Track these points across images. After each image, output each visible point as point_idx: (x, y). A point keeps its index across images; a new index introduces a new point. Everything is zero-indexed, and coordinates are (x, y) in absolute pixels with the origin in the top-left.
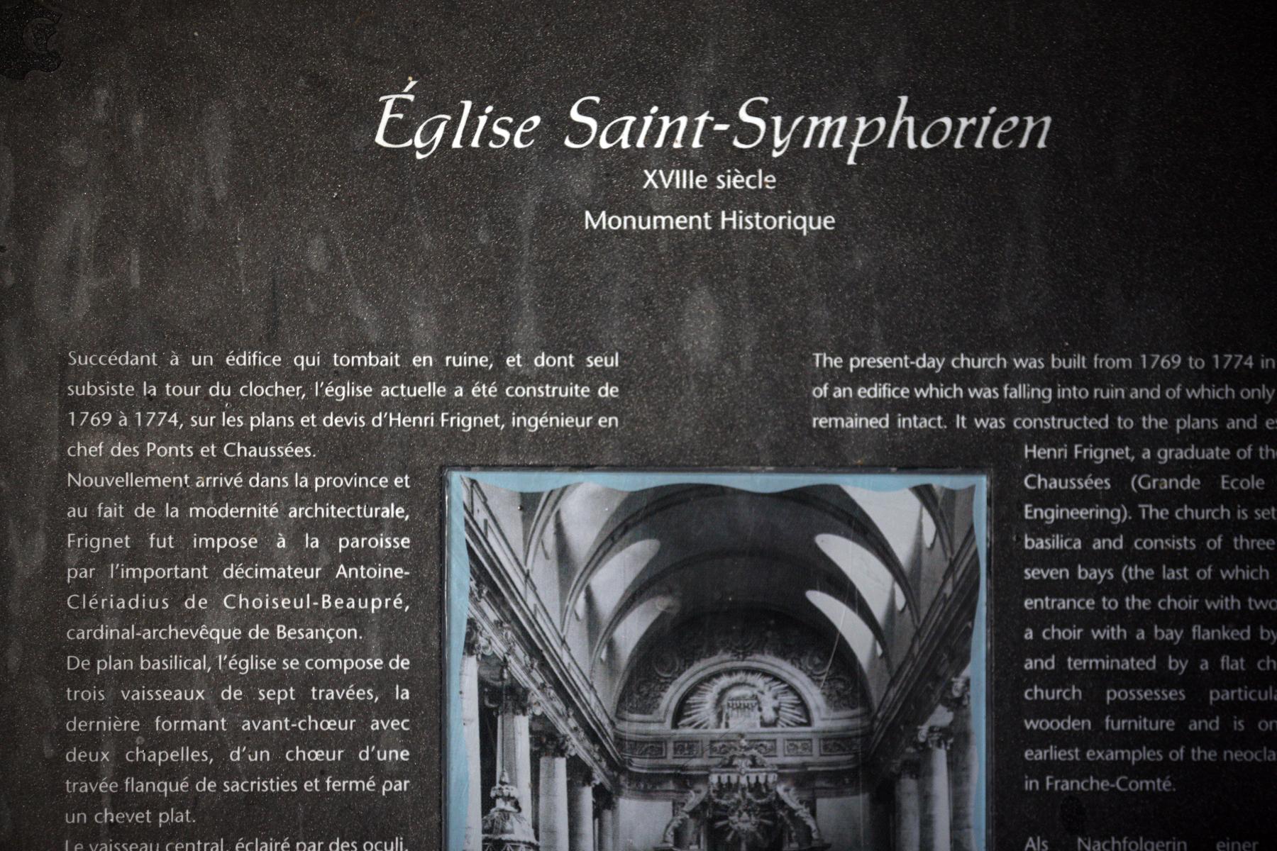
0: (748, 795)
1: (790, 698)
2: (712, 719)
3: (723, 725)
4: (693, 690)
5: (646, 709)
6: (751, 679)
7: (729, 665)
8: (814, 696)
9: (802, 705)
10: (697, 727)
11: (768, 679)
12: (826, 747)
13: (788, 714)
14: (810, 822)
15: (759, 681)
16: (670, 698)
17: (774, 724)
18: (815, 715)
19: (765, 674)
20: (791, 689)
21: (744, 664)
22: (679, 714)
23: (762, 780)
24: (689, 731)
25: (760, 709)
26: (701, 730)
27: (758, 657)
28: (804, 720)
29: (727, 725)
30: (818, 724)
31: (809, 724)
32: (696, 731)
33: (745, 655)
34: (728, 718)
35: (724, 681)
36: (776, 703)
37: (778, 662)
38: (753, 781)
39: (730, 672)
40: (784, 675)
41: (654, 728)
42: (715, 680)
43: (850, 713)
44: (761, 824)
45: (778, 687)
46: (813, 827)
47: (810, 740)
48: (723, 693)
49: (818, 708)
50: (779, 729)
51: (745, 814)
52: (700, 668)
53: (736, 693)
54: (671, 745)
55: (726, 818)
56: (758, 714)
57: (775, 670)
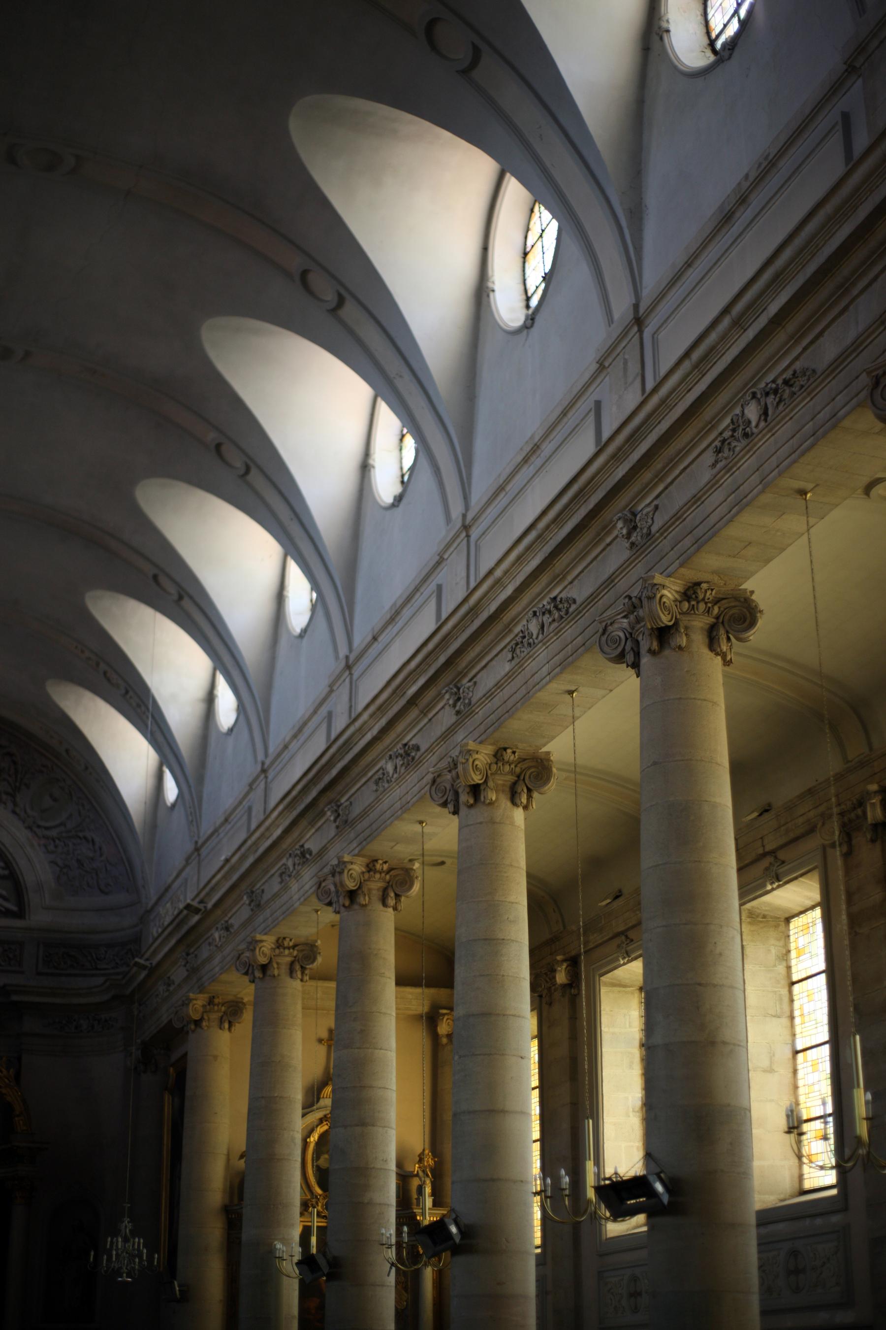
28: (15, 908)
30: (39, 917)
31: (20, 914)
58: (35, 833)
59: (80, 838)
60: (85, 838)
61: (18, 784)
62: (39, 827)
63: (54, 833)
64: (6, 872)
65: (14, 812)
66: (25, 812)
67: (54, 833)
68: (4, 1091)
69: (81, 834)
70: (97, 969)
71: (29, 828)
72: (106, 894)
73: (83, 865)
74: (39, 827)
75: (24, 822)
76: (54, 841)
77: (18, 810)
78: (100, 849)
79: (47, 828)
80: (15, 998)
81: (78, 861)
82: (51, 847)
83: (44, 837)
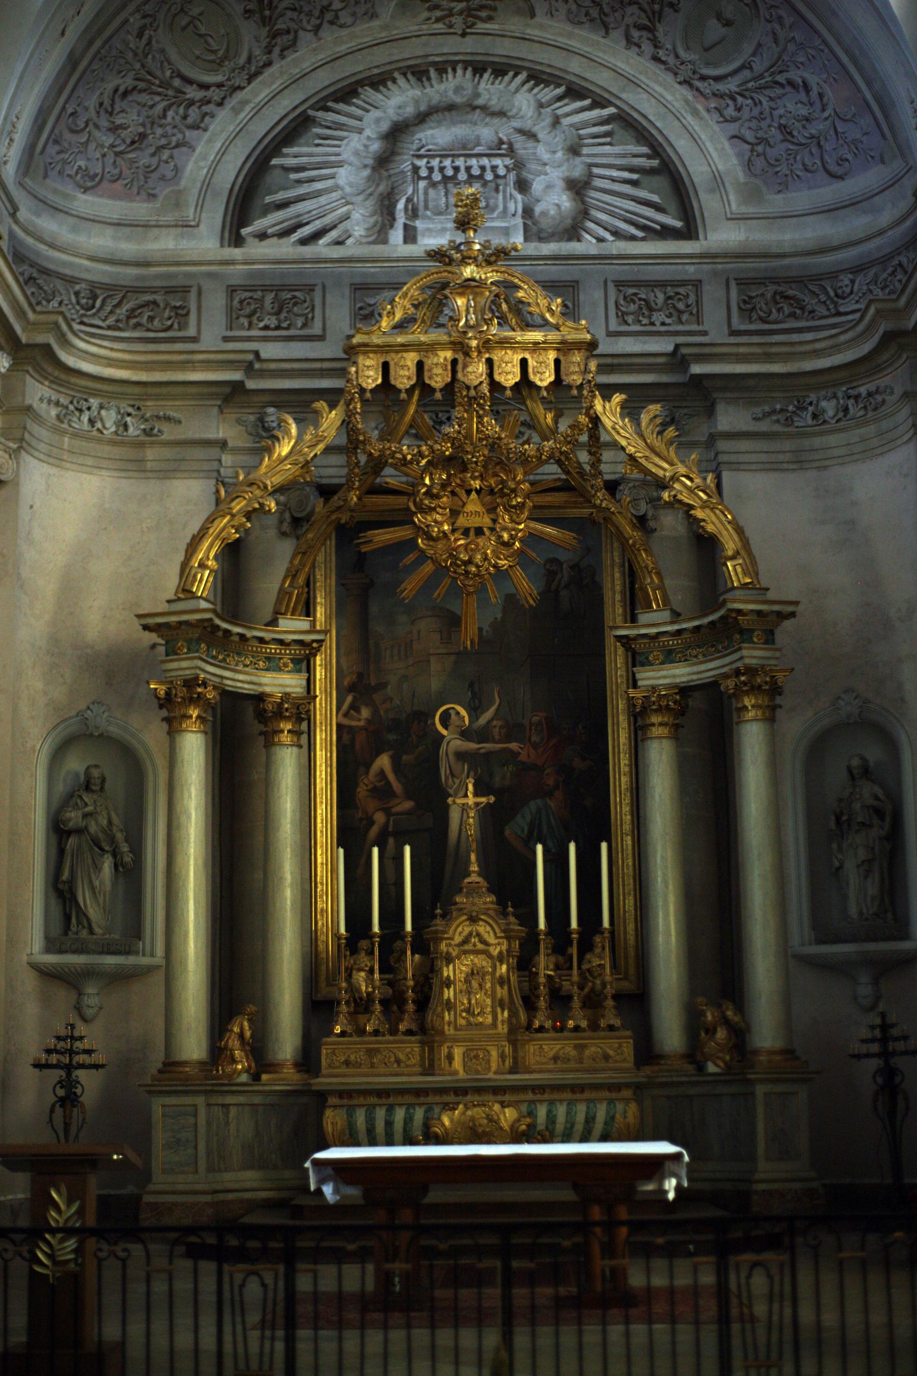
0: (492, 426)
1: (632, 150)
2: (360, 221)
3: (396, 236)
4: (295, 129)
5: (143, 185)
6: (490, 90)
7: (411, 51)
8: (707, 149)
9: (667, 172)
10: (304, 242)
11: (548, 93)
12: (748, 309)
13: (614, 201)
14: (713, 522)
15: (524, 102)
16: (215, 153)
17: (573, 232)
18: (708, 203)
19: (537, 78)
20: (629, 124)
21: (469, 46)
22: (243, 206)
23: (544, 378)
24: (286, 248)
25: (523, 186)
26: (322, 248)
27: (515, 25)
28: (678, 224)
29: (410, 236)
30: (722, 236)
31: (689, 232)
32: (308, 251)
33: (471, 14)
34: (413, 213)
35: (400, 100)
36: (577, 170)
37: (583, 39)
38: (509, 377)
39: (419, 73)
40: (601, 79)
41: (165, 244)
42: (368, 93)
43: (830, 192)
44: (532, 539)
45: (577, 115)
46: (730, 544)
47: (697, 284)
48: (396, 134)
49: (717, 182)
50: (587, 245)
51: (473, 505)
52: (316, 60)
53: (438, 135)
54: (216, 303)
55: (404, 518)
56: (517, 202)
57: (575, 66)
58: (698, 90)
59: (782, 86)
60: (790, 83)
61: (657, 7)
62: (703, 78)
63: (731, 85)
64: (655, 163)
65: (656, 59)
66: (677, 56)
67: (731, 85)
68: (699, 514)
69: (780, 78)
70: (839, 314)
71: (686, 82)
72: (841, 178)
73: (790, 134)
74: (703, 78)
75: (676, 74)
76: (734, 100)
77: (661, 54)
78: (821, 96)
79: (717, 79)
80: (696, 369)
81: (782, 128)
82: (730, 112)
83: (714, 95)
